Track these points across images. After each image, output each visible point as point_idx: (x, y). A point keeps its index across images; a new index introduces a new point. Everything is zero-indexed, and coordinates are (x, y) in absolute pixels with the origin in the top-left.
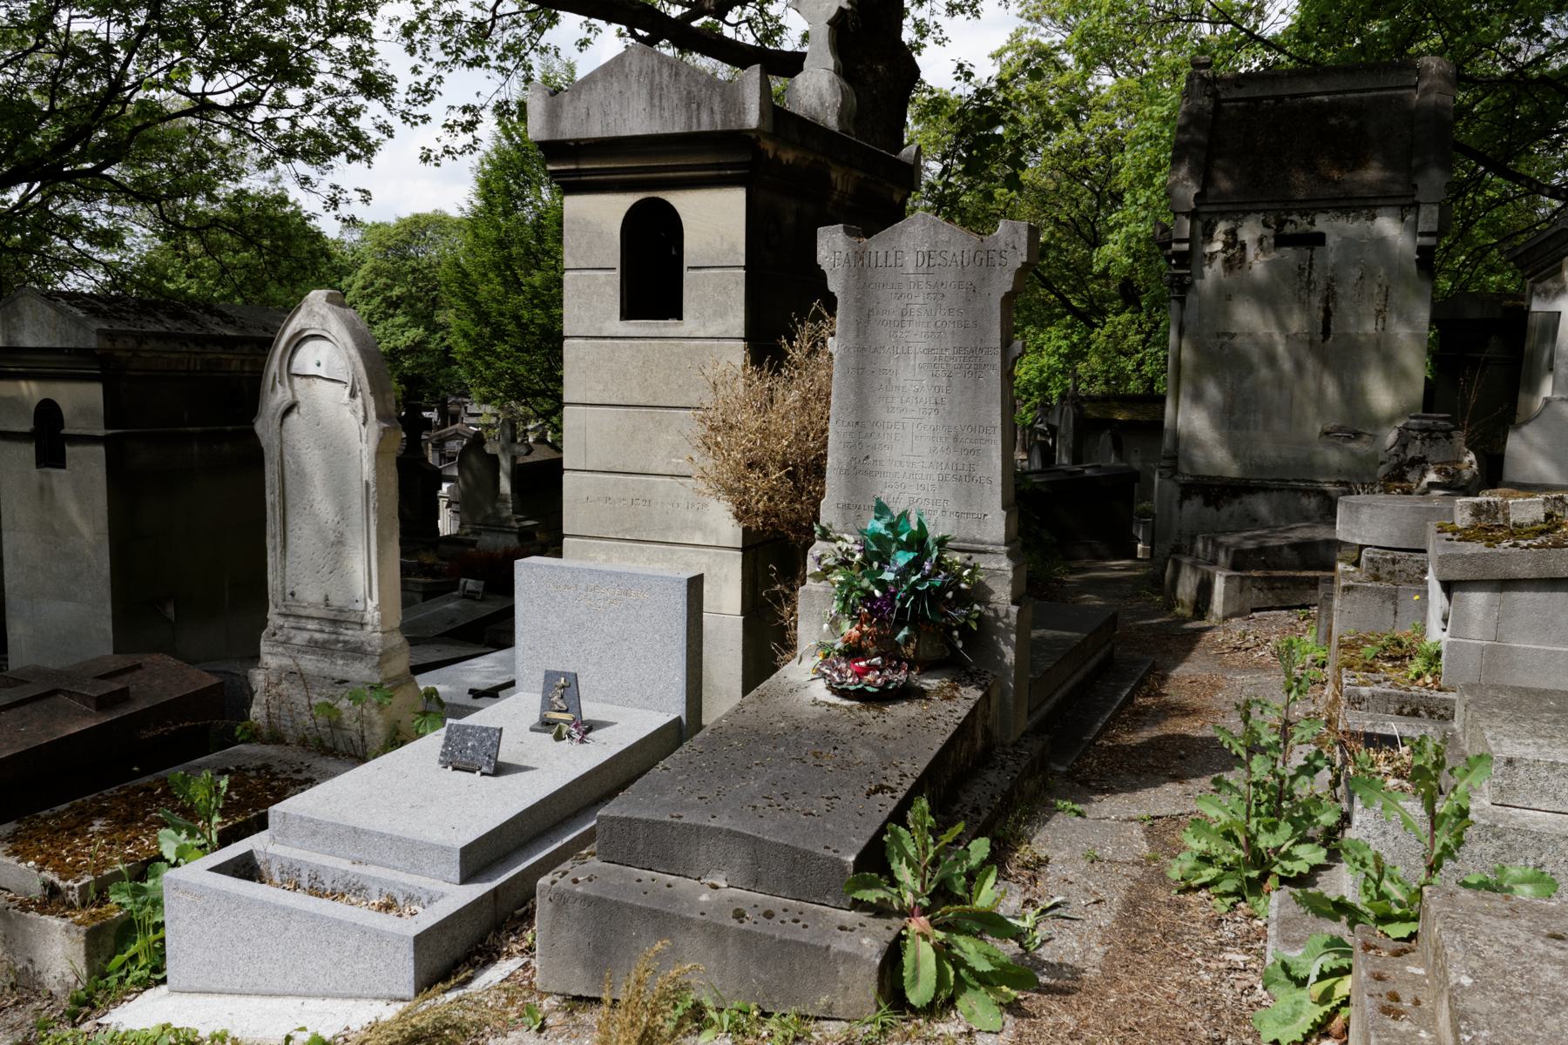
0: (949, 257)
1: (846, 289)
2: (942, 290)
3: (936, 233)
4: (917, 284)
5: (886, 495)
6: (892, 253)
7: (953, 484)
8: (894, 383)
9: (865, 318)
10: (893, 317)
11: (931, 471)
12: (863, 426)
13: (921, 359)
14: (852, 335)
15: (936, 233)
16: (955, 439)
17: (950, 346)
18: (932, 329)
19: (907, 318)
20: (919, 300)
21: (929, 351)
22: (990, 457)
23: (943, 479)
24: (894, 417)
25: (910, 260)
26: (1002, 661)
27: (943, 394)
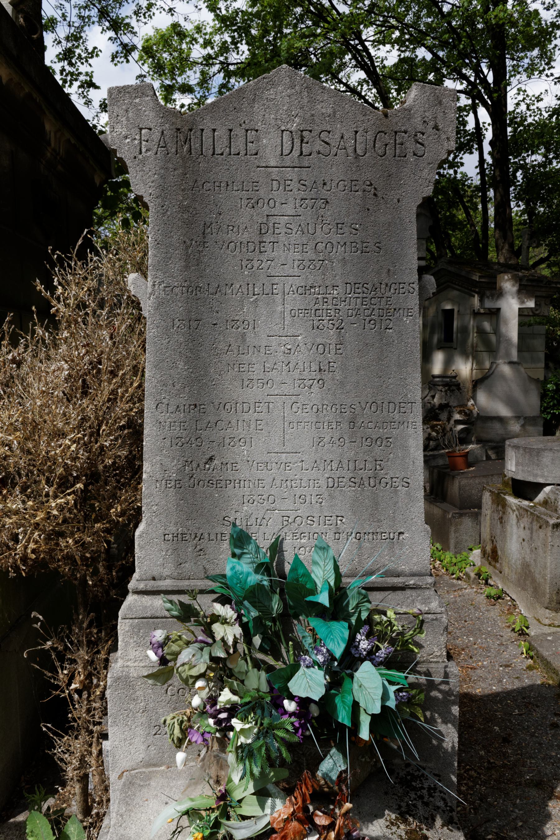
0: (334, 139)
1: (163, 192)
2: (324, 193)
3: (312, 101)
4: (284, 183)
5: (244, 511)
6: (239, 132)
7: (349, 491)
8: (250, 339)
9: (196, 238)
10: (245, 237)
11: (314, 474)
12: (201, 410)
13: (294, 301)
14: (176, 266)
15: (312, 101)
16: (352, 422)
17: (339, 281)
18: (310, 255)
19: (268, 238)
20: (287, 207)
21: (307, 289)
22: (405, 448)
23: (334, 485)
24: (254, 393)
25: (270, 146)
26: (440, 746)
27: (331, 356)
